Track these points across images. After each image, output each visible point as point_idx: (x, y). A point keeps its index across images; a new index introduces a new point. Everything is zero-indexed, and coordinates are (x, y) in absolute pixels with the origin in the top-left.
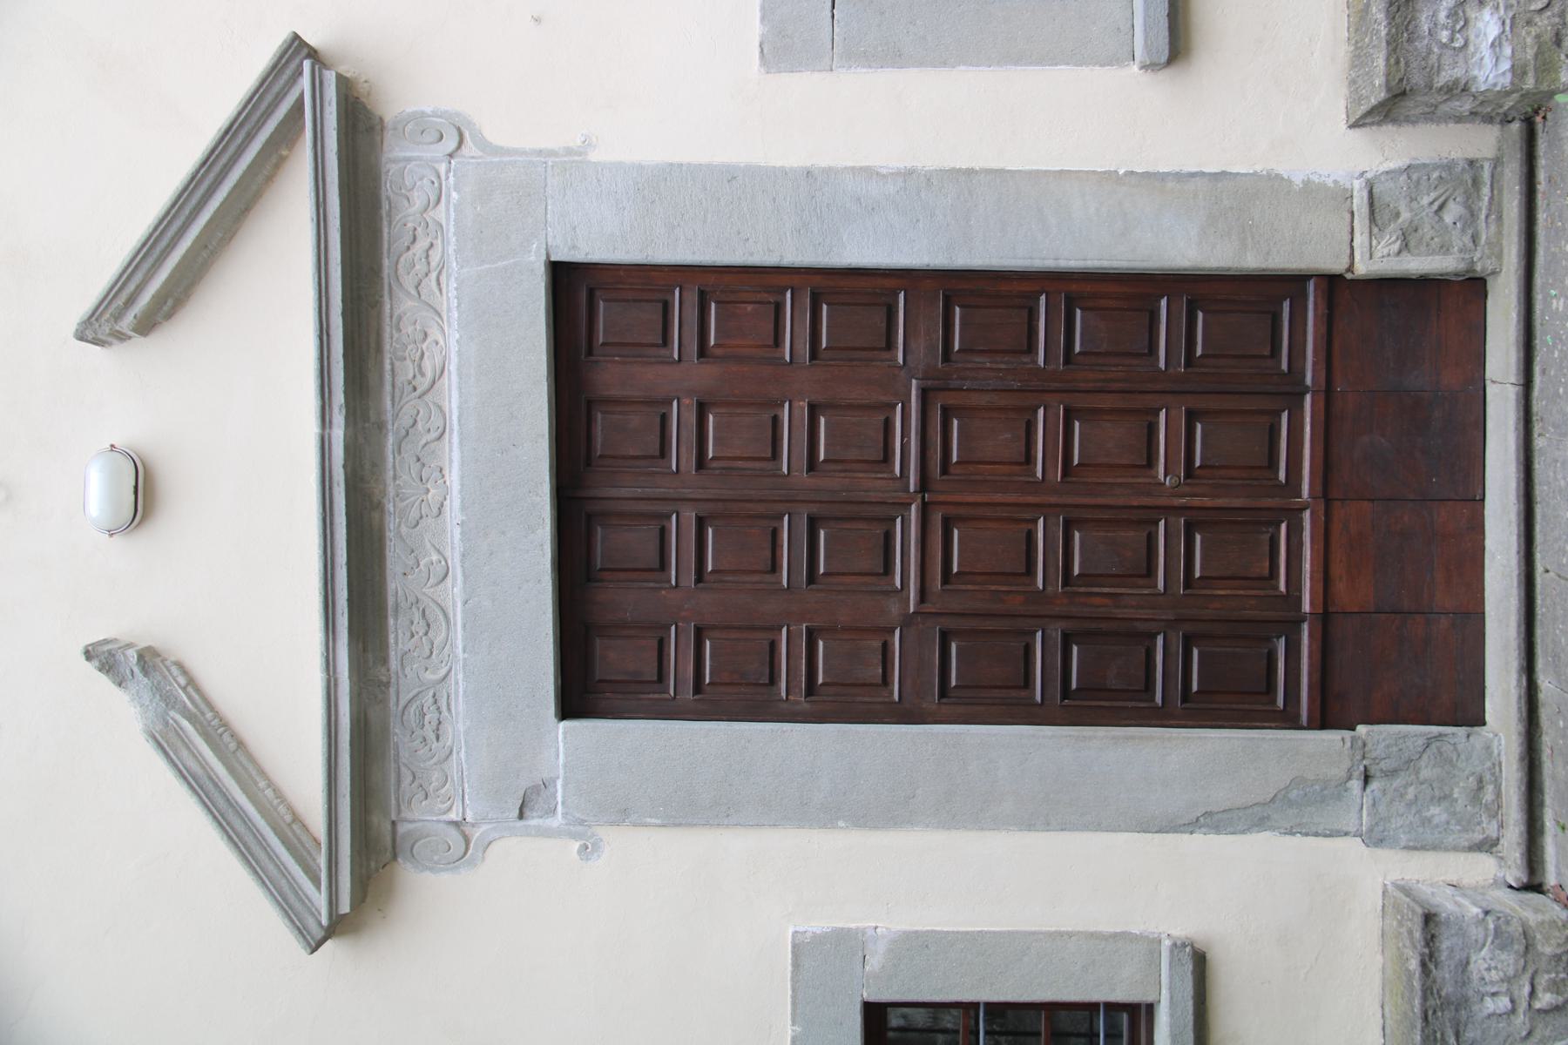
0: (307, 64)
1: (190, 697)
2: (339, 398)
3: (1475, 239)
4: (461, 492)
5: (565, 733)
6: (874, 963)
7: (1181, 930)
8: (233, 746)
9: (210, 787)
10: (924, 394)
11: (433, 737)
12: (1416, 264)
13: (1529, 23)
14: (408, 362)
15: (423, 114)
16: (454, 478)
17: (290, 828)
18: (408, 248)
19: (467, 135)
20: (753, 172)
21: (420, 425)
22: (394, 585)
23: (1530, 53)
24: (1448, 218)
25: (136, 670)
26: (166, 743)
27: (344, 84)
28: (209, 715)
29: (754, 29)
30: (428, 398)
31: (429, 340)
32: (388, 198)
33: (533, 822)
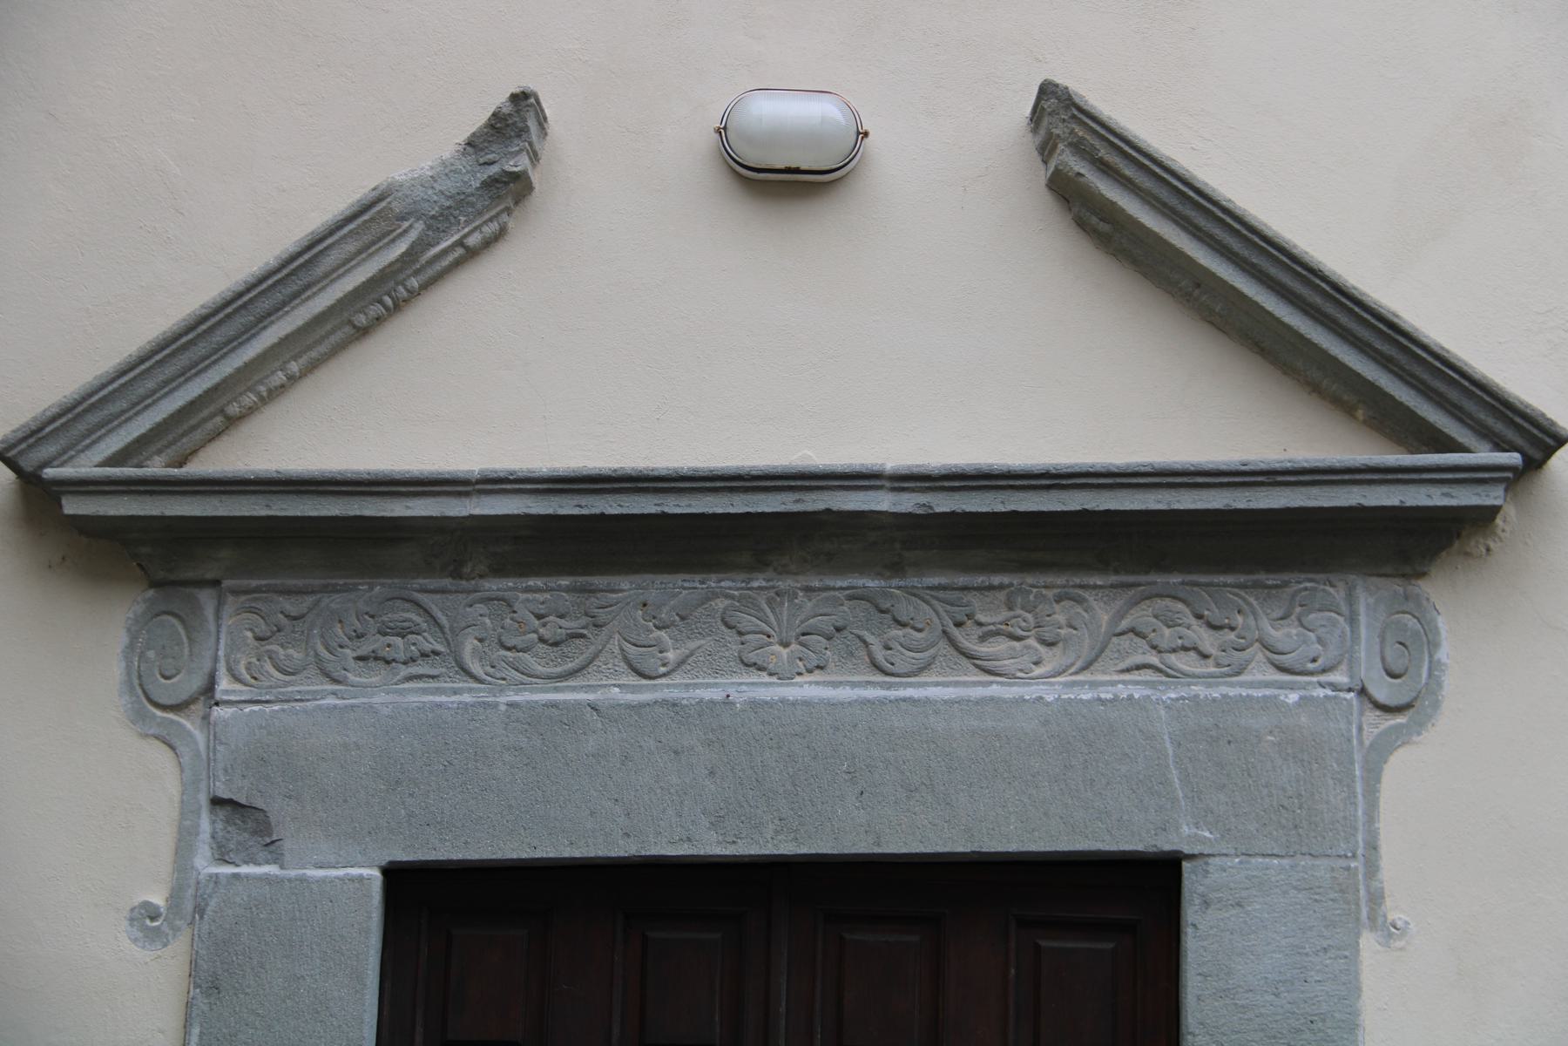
0: (1514, 458)
1: (445, 252)
2: (944, 503)
4: (783, 701)
5: (361, 879)
8: (361, 320)
9: (293, 288)
11: (365, 649)
14: (1004, 614)
15: (1433, 645)
16: (807, 689)
18: (1199, 617)
19: (1400, 720)
21: (898, 632)
22: (627, 586)
25: (494, 169)
27: (1484, 517)
28: (414, 283)
30: (943, 646)
31: (1042, 649)
32: (1286, 584)
33: (205, 824)
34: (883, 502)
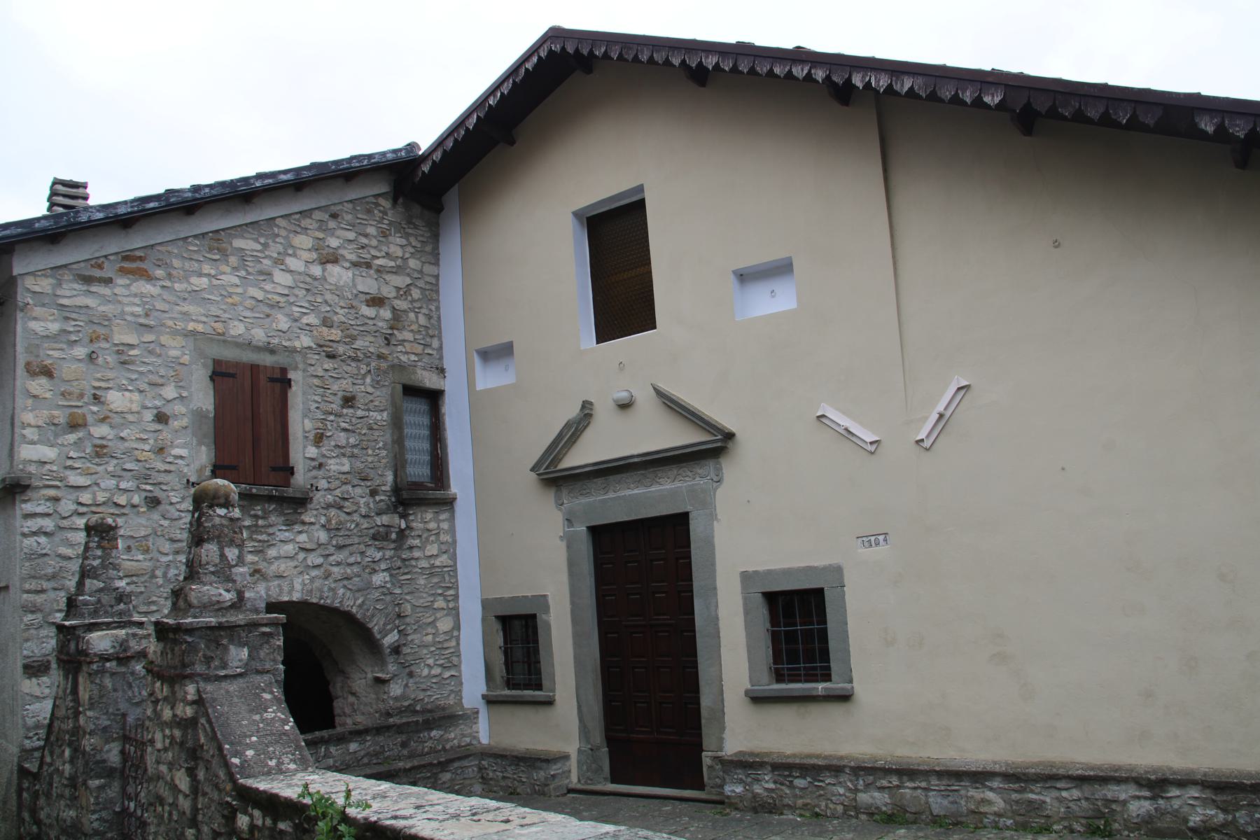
2: (644, 459)
3: (712, 787)
6: (544, 616)
7: (557, 698)
12: (705, 769)
13: (741, 801)
16: (636, 491)
17: (557, 460)
20: (714, 571)
22: (611, 477)
23: (733, 801)
24: (717, 780)
26: (568, 425)
29: (751, 569)
33: (566, 522)
34: (636, 460)
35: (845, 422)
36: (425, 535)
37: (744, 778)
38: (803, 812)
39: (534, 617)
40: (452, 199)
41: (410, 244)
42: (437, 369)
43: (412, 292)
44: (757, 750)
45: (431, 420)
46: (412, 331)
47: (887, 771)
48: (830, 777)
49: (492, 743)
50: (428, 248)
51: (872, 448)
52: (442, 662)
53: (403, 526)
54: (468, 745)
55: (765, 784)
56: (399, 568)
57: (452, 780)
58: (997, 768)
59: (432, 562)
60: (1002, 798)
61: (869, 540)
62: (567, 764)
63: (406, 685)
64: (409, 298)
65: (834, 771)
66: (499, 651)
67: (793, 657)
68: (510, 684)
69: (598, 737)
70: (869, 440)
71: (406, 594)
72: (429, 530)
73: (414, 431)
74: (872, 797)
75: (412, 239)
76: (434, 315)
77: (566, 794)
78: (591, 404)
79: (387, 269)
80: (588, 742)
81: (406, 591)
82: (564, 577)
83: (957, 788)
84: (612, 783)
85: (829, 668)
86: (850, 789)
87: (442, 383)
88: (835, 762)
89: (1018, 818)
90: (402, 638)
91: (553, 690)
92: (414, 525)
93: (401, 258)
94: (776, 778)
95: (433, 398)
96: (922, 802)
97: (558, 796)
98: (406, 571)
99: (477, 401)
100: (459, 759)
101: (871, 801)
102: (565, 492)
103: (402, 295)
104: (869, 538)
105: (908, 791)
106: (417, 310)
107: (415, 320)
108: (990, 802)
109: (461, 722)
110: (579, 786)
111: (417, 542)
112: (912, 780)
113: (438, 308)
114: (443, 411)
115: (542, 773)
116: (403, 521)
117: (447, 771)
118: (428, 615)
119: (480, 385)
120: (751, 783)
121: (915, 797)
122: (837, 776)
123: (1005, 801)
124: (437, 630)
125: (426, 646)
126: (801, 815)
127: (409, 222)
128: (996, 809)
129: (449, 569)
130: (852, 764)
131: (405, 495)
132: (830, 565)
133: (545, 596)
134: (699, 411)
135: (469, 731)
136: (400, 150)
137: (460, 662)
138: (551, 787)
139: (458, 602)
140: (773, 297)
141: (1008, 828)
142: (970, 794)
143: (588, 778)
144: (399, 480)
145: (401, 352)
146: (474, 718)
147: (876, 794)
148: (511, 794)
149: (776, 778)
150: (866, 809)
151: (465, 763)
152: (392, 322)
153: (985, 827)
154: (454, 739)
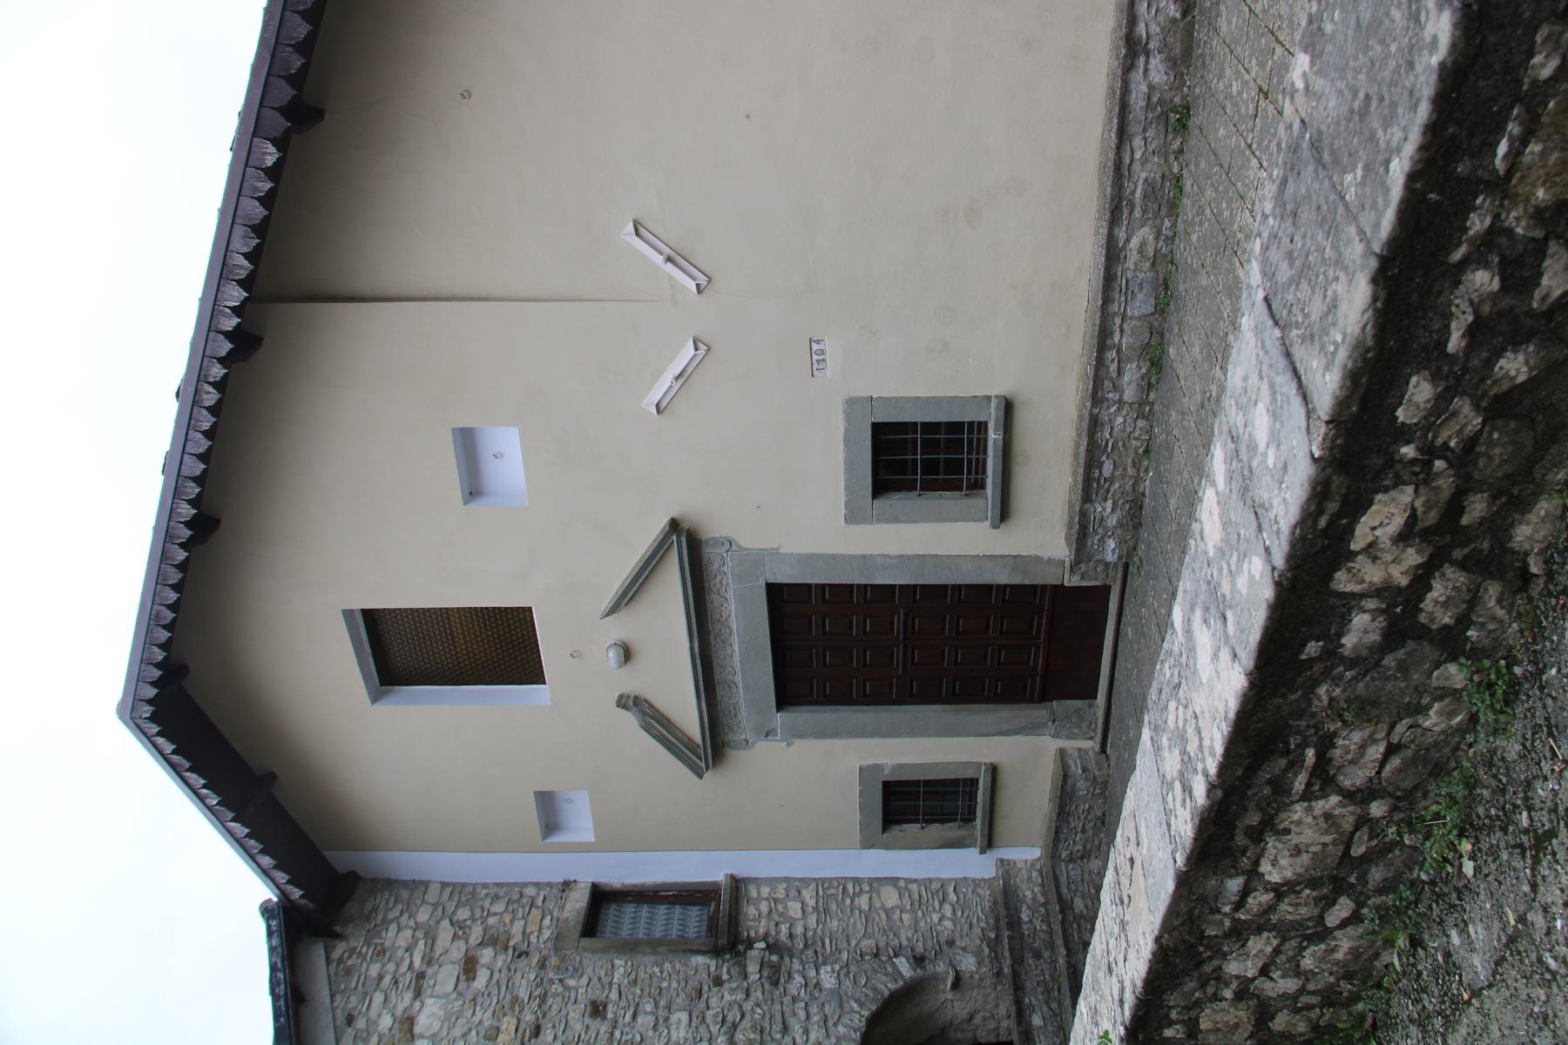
2: (695, 634)
3: (1107, 576)
6: (886, 772)
7: (987, 761)
10: (906, 615)
12: (1084, 584)
16: (736, 647)
17: (689, 744)
20: (842, 556)
22: (716, 678)
24: (1099, 569)
26: (647, 728)
29: (843, 511)
33: (769, 738)
34: (696, 645)
35: (666, 381)
36: (776, 918)
37: (1098, 537)
38: (1142, 469)
39: (886, 785)
40: (342, 860)
41: (397, 918)
42: (563, 891)
43: (461, 919)
44: (1066, 517)
45: (630, 902)
46: (512, 921)
47: (1100, 363)
48: (1102, 431)
49: (1041, 843)
50: (405, 894)
51: (703, 348)
52: (936, 902)
53: (762, 945)
54: (1041, 874)
55: (1108, 512)
56: (816, 952)
57: (1083, 897)
58: (1104, 231)
59: (811, 909)
60: (1139, 229)
61: (817, 361)
62: (1070, 752)
63: (964, 949)
64: (468, 923)
65: (1095, 428)
66: (927, 829)
67: (955, 467)
68: (969, 818)
69: (1039, 713)
70: (692, 352)
71: (849, 945)
72: (770, 911)
73: (643, 924)
74: (1129, 384)
75: (391, 915)
76: (493, 891)
77: (1107, 756)
78: (621, 696)
79: (428, 951)
80: (1045, 725)
81: (846, 945)
82: (838, 744)
83: (1124, 281)
84: (1096, 698)
85: (971, 424)
86: (1119, 409)
87: (583, 885)
88: (1085, 425)
89: (1164, 212)
90: (904, 952)
91: (979, 765)
92: (761, 931)
93: (415, 930)
94: (1100, 498)
95: (601, 897)
96: (1139, 324)
97: (1109, 765)
98: (820, 943)
99: (608, 842)
100: (1057, 886)
101: (1134, 385)
102: (731, 737)
103: (464, 933)
104: (814, 361)
105: (1125, 340)
106: (485, 914)
107: (498, 917)
108: (1143, 244)
109: (1012, 882)
110: (1098, 738)
111: (784, 928)
112: (1111, 334)
113: (485, 886)
114: (618, 886)
115: (1080, 784)
116: (756, 945)
117: (1072, 903)
118: (877, 918)
119: (589, 836)
120: (1104, 528)
121: (1132, 332)
122: (1102, 425)
123: (1142, 226)
124: (897, 906)
125: (916, 922)
126: (1147, 471)
127: (368, 918)
128: (1151, 237)
129: (820, 888)
130: (1089, 404)
131: (723, 941)
132: (844, 412)
133: (861, 769)
134: (640, 560)
135: (1024, 872)
136: (269, 927)
137: (938, 879)
138: (1097, 773)
139: (863, 879)
140: (502, 455)
141: (1174, 225)
142: (1132, 267)
143: (1089, 727)
144: (703, 948)
145: (538, 937)
146: (1009, 864)
147: (1126, 378)
148: (1103, 823)
149: (1100, 498)
150: (1143, 392)
151: (1063, 879)
152: (498, 948)
153: (1172, 252)
154: (1033, 891)
